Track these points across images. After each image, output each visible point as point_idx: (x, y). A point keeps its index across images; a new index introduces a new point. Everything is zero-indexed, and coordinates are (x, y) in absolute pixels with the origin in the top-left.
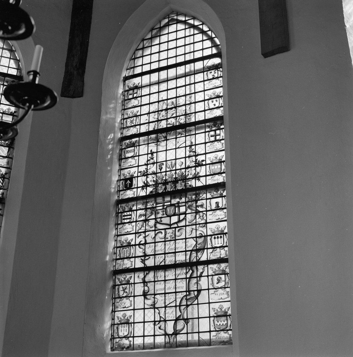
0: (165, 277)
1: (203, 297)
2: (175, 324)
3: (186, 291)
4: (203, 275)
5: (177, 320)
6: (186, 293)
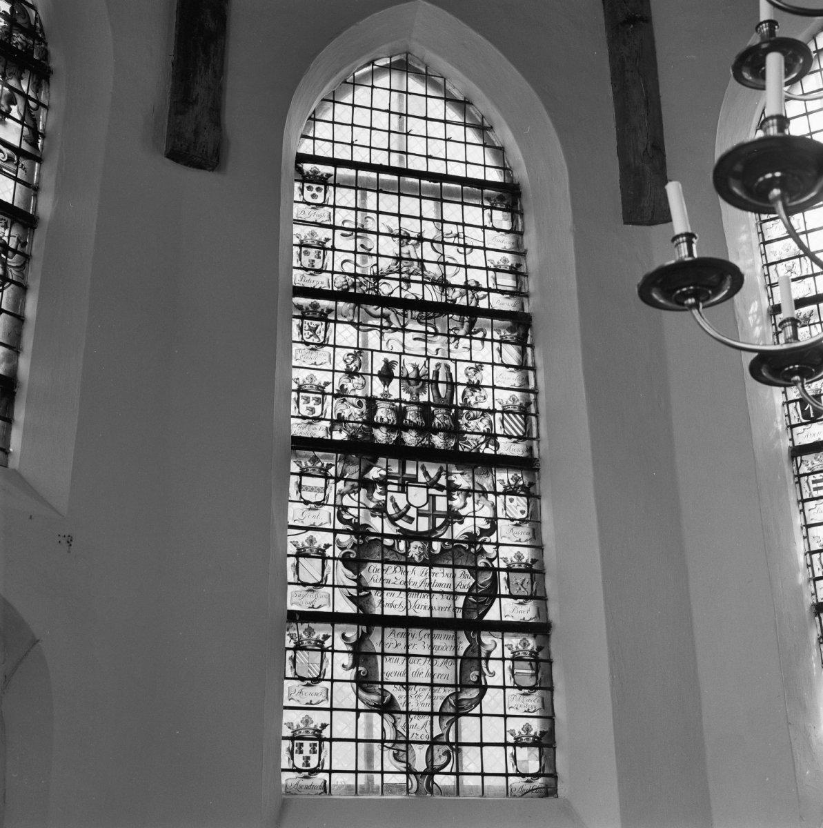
0: (407, 647)
1: (492, 701)
2: (430, 750)
5: (433, 742)
6: (457, 689)
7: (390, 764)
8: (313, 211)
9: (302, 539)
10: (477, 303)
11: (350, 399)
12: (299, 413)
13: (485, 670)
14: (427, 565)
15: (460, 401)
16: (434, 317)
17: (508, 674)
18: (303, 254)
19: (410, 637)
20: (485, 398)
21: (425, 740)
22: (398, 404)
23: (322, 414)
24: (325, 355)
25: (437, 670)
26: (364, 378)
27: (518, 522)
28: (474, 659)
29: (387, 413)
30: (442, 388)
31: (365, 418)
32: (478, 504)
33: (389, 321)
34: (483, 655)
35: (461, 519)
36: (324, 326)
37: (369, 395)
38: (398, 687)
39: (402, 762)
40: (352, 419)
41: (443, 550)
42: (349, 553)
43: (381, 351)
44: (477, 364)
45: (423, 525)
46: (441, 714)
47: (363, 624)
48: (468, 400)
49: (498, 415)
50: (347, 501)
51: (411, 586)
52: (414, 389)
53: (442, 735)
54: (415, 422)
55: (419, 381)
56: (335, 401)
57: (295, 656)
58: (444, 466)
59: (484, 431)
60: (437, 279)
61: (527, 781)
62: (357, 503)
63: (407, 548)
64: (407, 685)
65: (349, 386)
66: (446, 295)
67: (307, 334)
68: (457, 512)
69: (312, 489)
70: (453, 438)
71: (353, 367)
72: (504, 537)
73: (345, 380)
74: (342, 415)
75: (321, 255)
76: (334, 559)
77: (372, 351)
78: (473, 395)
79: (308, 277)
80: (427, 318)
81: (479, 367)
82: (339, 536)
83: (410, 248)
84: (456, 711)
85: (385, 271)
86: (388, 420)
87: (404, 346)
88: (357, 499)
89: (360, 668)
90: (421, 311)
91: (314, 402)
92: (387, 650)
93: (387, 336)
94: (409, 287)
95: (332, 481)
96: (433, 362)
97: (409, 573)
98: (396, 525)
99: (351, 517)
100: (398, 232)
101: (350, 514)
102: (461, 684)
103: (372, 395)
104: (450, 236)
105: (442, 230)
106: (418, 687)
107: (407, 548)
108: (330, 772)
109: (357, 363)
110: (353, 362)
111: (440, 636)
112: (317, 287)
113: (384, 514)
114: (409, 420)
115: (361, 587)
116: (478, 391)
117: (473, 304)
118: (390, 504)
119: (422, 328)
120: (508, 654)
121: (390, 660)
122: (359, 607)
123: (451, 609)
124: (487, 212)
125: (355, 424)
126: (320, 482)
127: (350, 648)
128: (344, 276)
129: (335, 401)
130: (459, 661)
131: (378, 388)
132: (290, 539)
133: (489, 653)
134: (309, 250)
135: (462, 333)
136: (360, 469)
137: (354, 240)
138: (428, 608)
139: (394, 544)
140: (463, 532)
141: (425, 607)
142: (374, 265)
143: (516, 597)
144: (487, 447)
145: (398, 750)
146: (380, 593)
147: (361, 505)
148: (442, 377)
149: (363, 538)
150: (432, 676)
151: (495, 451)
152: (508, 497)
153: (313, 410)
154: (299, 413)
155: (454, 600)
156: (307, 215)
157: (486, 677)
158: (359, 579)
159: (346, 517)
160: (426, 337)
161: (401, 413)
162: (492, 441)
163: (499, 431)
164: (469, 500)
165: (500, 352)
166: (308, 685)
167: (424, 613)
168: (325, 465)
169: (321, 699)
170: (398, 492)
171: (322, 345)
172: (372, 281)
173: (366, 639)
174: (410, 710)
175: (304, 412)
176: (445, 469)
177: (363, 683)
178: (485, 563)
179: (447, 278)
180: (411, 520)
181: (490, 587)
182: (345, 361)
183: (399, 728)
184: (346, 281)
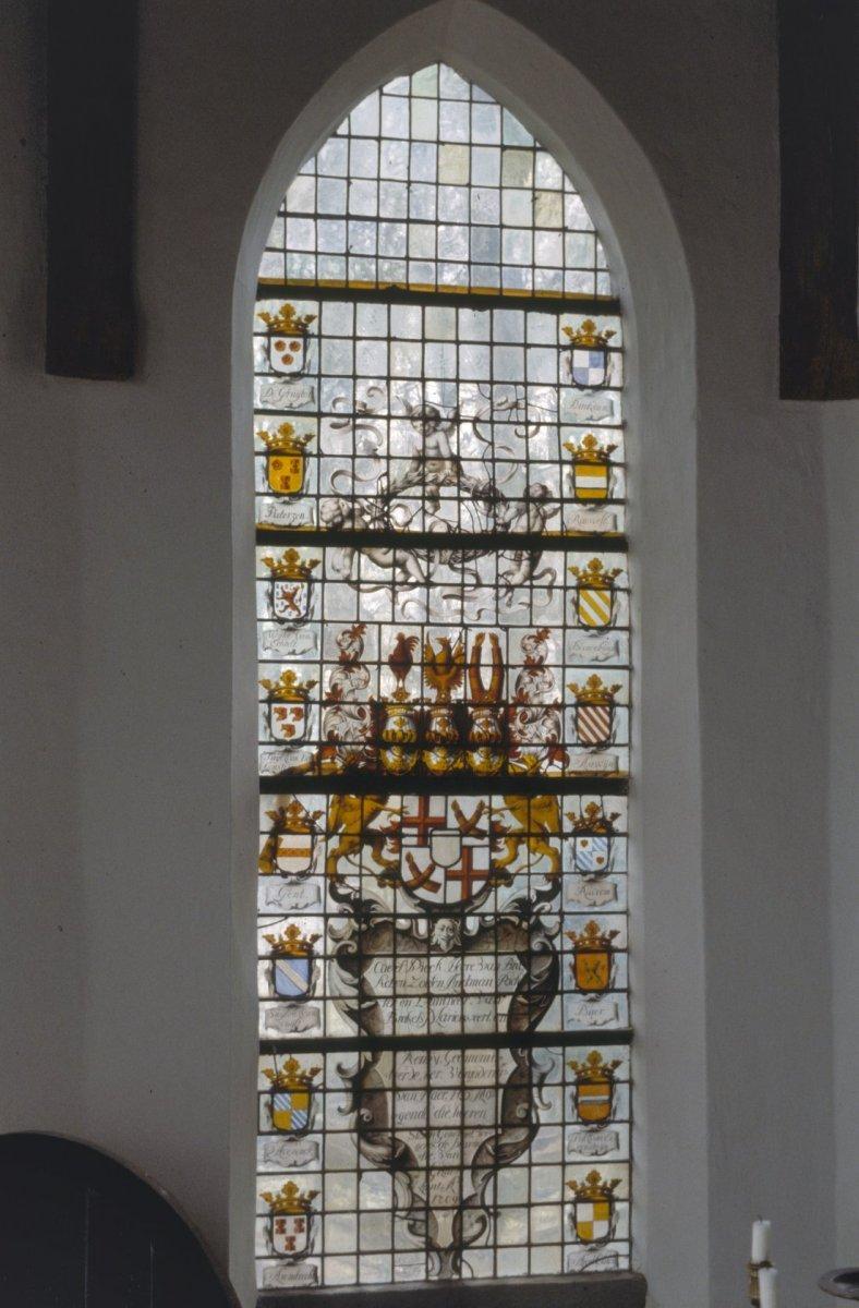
0: (429, 1076)
1: (547, 1145)
2: (458, 1220)
3: (495, 1126)
4: (547, 1081)
5: (463, 1205)
7: (407, 1239)
8: (286, 388)
9: (279, 930)
10: (543, 526)
11: (346, 707)
12: (271, 735)
13: (537, 1100)
14: (456, 956)
15: (513, 693)
16: (475, 557)
17: (569, 1103)
18: (271, 468)
19: (433, 1062)
20: (550, 685)
21: (451, 1203)
22: (418, 708)
23: (304, 735)
24: (308, 637)
25: (471, 1106)
26: (366, 669)
27: (592, 876)
28: (520, 1088)
29: (402, 723)
30: (487, 677)
31: (369, 734)
32: (534, 854)
33: (406, 573)
34: (535, 1081)
35: (508, 879)
36: (305, 590)
37: (376, 699)
38: (415, 1133)
39: (419, 1235)
40: (349, 740)
41: (483, 929)
42: (347, 946)
43: (393, 623)
44: (540, 630)
45: (454, 892)
46: (475, 1168)
47: (366, 1050)
48: (525, 691)
49: (570, 712)
50: (343, 866)
51: (434, 990)
52: (443, 680)
53: (476, 1195)
54: (444, 734)
55: (447, 667)
56: (324, 712)
57: (273, 1101)
58: (485, 799)
59: (547, 739)
60: (481, 488)
61: (592, 1250)
62: (358, 869)
63: (430, 930)
64: (427, 1131)
65: (346, 686)
66: (495, 516)
67: (280, 604)
68: (503, 869)
69: (293, 853)
70: (500, 755)
71: (351, 652)
72: (573, 900)
73: (339, 676)
74: (336, 732)
75: (300, 467)
76: (326, 958)
77: (380, 624)
78: (532, 681)
79: (280, 509)
80: (465, 559)
81: (542, 636)
82: (332, 921)
83: (439, 437)
84: (499, 1158)
85: (399, 484)
86: (404, 734)
87: (428, 610)
88: (357, 862)
89: (364, 1111)
90: (455, 549)
91: (293, 715)
92: (400, 1083)
93: (402, 596)
94: (437, 508)
95: (320, 837)
96: (473, 634)
97: (432, 970)
98: (415, 897)
99: (350, 891)
100: (420, 409)
101: (348, 887)
102: (506, 1123)
103: (379, 697)
104: (503, 407)
105: (491, 398)
106: (443, 1132)
107: (430, 930)
108: (323, 1255)
109: (356, 645)
110: (350, 644)
111: (475, 1059)
112: (295, 523)
113: (398, 882)
114: (435, 732)
115: (364, 994)
116: (540, 673)
117: (536, 528)
118: (405, 867)
119: (456, 578)
120: (571, 1077)
121: (404, 1096)
122: (362, 1025)
123: (491, 1017)
124: (565, 354)
125: (354, 747)
126: (303, 841)
127: (349, 1085)
128: (335, 499)
129: (324, 712)
130: (501, 1091)
131: (388, 684)
132: (261, 933)
133: (543, 1076)
134: (281, 459)
135: (517, 579)
136: (362, 816)
137: (351, 433)
138: (458, 1018)
139: (411, 926)
140: (513, 898)
141: (455, 1018)
142: (384, 475)
143: (584, 992)
144: (551, 763)
145: (415, 1220)
146: (391, 1002)
147: (364, 872)
148: (486, 657)
149: (366, 922)
150: (463, 1114)
151: (563, 769)
152: (579, 840)
153: (290, 729)
154: (271, 735)
155: (496, 1003)
156: (277, 397)
157: (540, 1112)
158: (361, 985)
159: (342, 891)
160: (463, 591)
161: (422, 721)
162: (559, 753)
163: (570, 738)
164: (523, 849)
165: (576, 604)
166: (291, 1140)
167: (452, 1028)
168: (311, 814)
169: (308, 1157)
170: (415, 846)
171: (301, 621)
172: (379, 505)
173: (371, 1070)
174: (431, 1164)
175: (280, 734)
176: (487, 804)
177: (366, 1131)
178: (542, 943)
179: (497, 486)
180: (435, 887)
181: (547, 980)
182: (339, 644)
183: (416, 1191)
184: (339, 508)
